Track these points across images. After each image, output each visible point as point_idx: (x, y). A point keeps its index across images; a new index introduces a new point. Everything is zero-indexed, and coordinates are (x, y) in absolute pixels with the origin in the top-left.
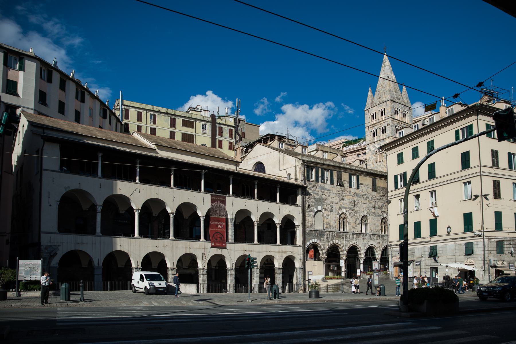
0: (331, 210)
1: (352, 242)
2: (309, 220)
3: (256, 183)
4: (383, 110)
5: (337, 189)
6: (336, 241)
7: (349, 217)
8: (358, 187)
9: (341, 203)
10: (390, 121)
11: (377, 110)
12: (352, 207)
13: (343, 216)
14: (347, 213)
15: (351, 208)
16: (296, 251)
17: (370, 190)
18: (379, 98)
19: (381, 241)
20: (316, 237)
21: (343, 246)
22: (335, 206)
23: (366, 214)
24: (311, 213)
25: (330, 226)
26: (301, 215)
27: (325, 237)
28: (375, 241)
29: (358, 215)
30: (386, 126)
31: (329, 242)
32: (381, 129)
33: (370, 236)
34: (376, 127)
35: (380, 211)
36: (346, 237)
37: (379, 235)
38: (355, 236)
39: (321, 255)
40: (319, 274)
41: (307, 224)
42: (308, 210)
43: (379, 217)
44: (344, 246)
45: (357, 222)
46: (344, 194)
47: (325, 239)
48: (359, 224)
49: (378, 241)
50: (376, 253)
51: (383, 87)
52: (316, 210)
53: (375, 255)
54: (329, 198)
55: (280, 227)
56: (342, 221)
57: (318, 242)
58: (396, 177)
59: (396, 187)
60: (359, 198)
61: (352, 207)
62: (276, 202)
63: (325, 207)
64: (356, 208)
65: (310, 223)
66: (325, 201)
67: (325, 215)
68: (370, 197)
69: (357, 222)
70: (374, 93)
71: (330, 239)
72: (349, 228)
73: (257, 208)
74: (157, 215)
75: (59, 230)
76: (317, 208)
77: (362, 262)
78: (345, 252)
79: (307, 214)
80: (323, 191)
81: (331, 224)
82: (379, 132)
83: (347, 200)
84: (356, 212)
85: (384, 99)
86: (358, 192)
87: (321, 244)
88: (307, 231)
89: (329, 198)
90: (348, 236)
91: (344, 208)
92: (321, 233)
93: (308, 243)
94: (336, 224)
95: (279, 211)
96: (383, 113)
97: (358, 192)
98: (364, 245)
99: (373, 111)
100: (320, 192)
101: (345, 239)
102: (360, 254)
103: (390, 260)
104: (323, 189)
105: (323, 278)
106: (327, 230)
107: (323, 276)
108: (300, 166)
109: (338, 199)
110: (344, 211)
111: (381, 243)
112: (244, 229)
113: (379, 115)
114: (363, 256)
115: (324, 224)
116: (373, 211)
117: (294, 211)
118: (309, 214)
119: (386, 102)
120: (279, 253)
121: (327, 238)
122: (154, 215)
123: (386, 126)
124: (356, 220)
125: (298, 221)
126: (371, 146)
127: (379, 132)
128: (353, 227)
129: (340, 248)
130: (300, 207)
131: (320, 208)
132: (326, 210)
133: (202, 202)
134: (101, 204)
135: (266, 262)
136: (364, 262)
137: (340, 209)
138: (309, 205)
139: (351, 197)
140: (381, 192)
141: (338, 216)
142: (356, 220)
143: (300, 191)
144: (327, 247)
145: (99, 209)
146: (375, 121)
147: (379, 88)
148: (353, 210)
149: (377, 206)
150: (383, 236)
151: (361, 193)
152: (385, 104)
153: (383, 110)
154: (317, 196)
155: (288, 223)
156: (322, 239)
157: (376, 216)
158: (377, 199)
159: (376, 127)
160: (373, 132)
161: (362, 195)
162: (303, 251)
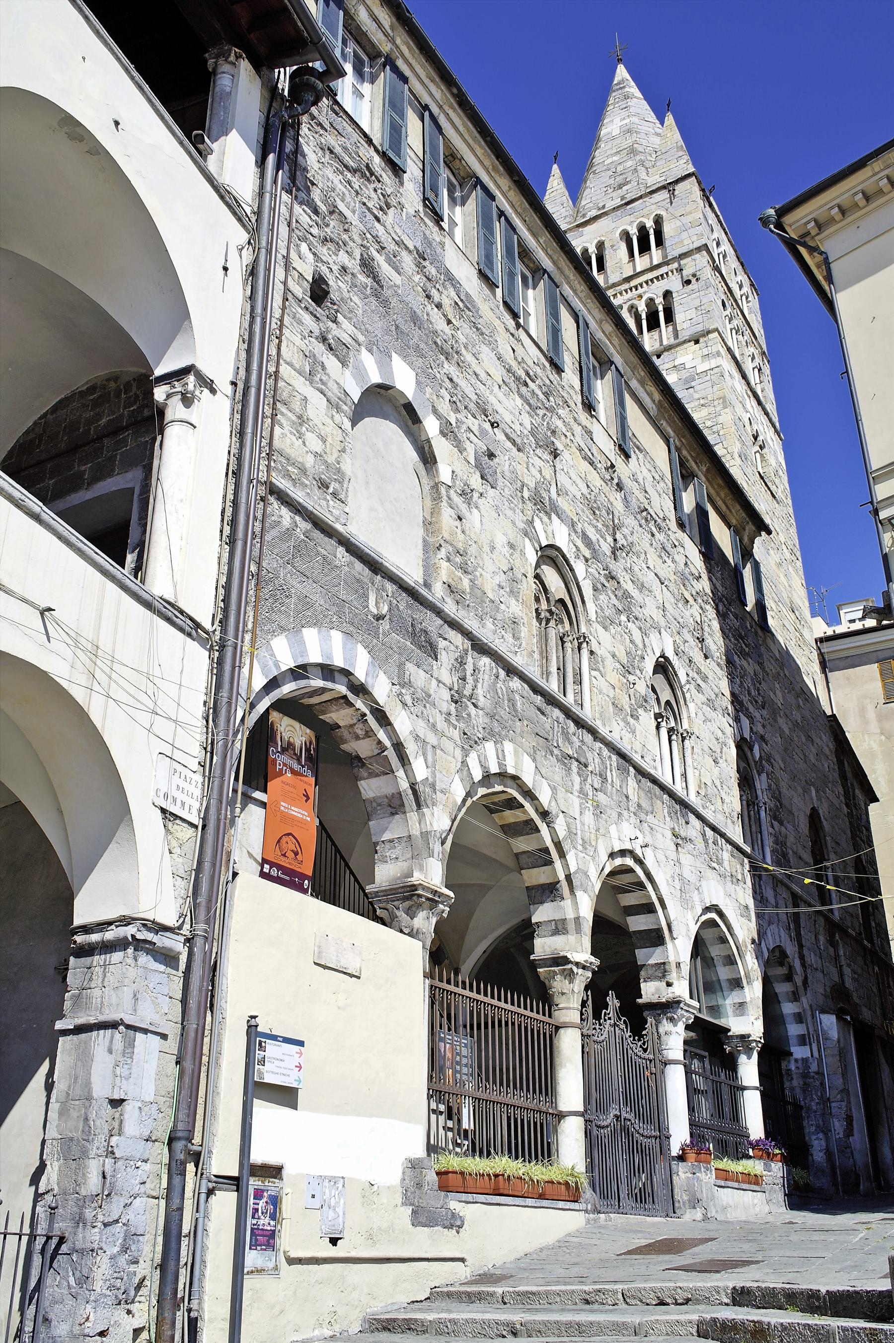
1: (623, 834)
4: (650, 224)
14: (580, 568)
18: (620, 187)
20: (364, 628)
24: (331, 362)
26: (236, 290)
27: (444, 668)
30: (673, 283)
31: (470, 742)
38: (632, 783)
40: (376, 1107)
63: (444, 407)
64: (617, 568)
70: (575, 187)
71: (479, 718)
78: (584, 906)
85: (655, 179)
93: (282, 653)
101: (577, 780)
110: (562, 538)
119: (669, 187)
123: (673, 283)
138: (319, 292)
144: (459, 792)
148: (611, 577)
153: (650, 224)
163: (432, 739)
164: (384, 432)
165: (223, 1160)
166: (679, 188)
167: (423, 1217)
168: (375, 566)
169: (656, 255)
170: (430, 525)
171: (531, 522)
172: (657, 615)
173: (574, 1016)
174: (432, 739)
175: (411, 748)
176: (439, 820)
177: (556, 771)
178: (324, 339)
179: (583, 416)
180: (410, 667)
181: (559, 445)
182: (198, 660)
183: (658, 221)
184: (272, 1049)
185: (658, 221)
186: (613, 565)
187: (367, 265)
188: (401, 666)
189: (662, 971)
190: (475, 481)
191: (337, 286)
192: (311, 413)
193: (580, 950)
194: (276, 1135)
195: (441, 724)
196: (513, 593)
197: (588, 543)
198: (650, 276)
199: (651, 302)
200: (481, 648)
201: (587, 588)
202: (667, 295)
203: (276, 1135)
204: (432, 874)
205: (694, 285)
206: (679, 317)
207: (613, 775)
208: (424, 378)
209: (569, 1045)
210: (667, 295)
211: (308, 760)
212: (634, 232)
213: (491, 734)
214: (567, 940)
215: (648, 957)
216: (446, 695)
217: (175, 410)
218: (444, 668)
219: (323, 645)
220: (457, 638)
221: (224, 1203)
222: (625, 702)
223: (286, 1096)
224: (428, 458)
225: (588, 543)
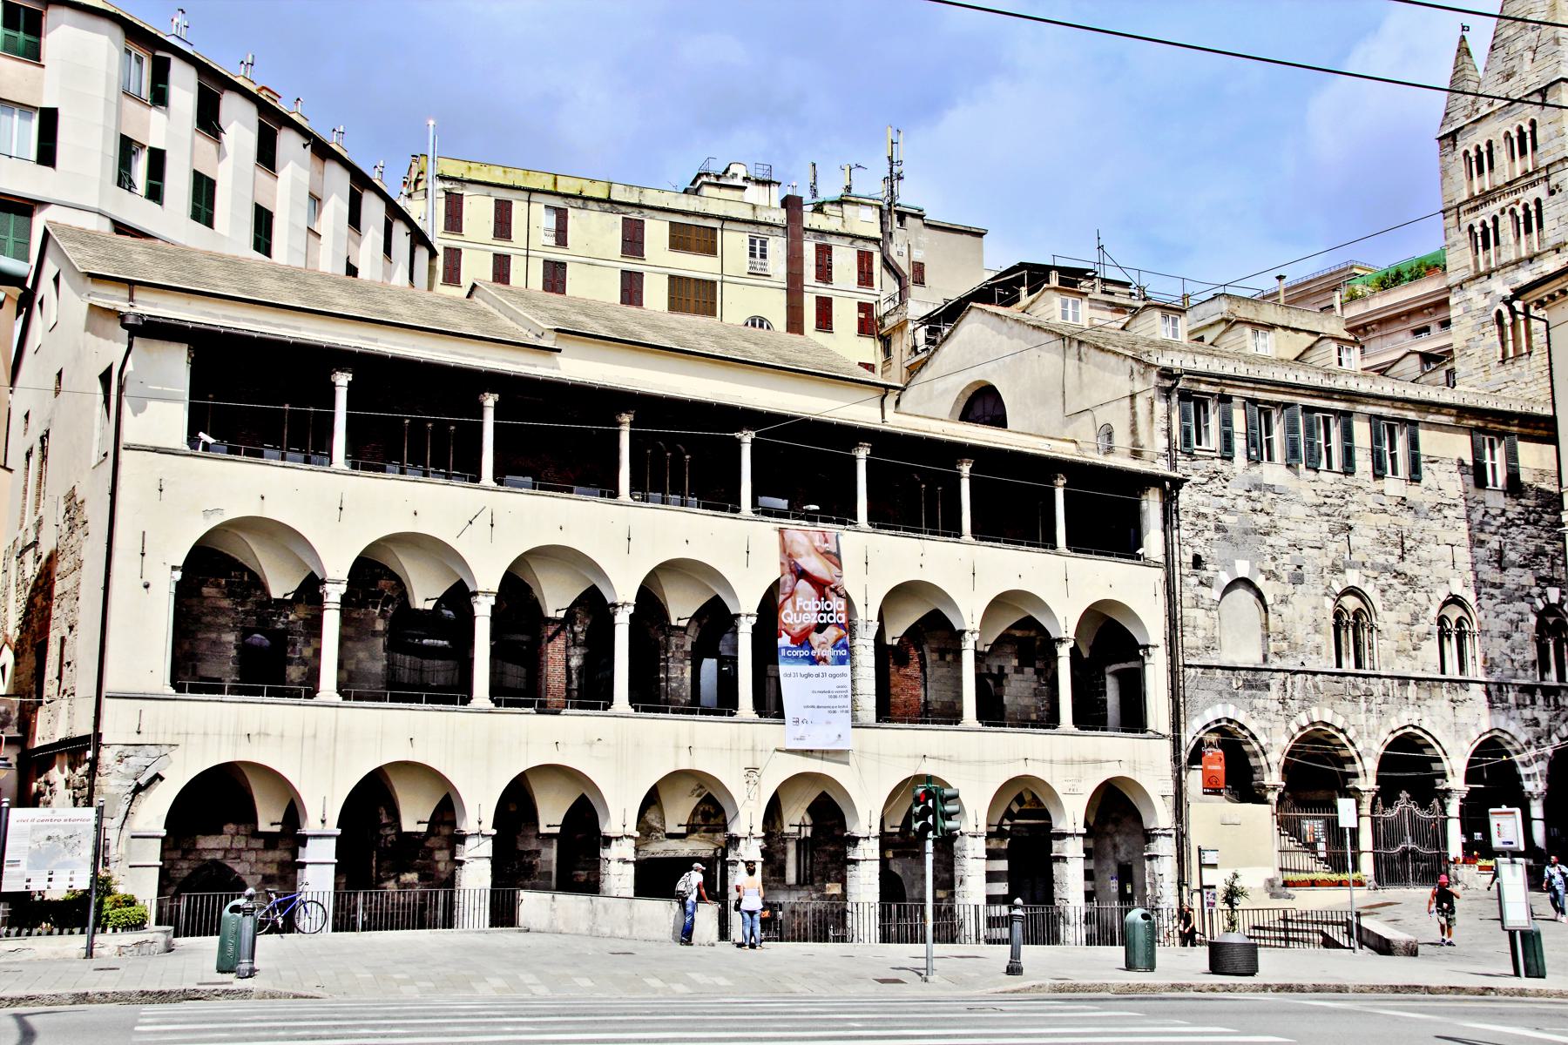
0: (1297, 579)
1: (1401, 718)
5: (1319, 486)
7: (1378, 606)
8: (1415, 475)
12: (1393, 560)
13: (1351, 603)
14: (1369, 589)
15: (1385, 569)
18: (1508, 77)
22: (1313, 561)
24: (1204, 591)
25: (1293, 646)
27: (1275, 692)
28: (1515, 713)
29: (1421, 597)
31: (1290, 717)
32: (1520, 212)
33: (1488, 693)
34: (1494, 208)
35: (1528, 578)
36: (1368, 695)
37: (1528, 690)
41: (1189, 640)
42: (1194, 581)
43: (1524, 606)
45: (1421, 628)
46: (1352, 507)
47: (1276, 706)
49: (1527, 713)
52: (1226, 579)
55: (1074, 652)
56: (1351, 626)
57: (1241, 718)
60: (1423, 523)
61: (1393, 560)
62: (1054, 547)
64: (1408, 567)
65: (1201, 633)
66: (1269, 540)
69: (1421, 628)
72: (1385, 653)
73: (971, 574)
74: (561, 615)
75: (174, 684)
79: (1187, 594)
80: (1255, 494)
83: (1363, 537)
84: (1411, 582)
86: (1414, 493)
87: (1253, 726)
88: (1190, 672)
89: (1282, 524)
91: (1352, 566)
92: (1254, 679)
94: (1318, 638)
95: (1066, 584)
96: (1524, 142)
97: (1414, 493)
100: (1241, 502)
101: (1363, 705)
104: (1257, 487)
106: (1276, 663)
108: (1152, 393)
109: (1325, 527)
110: (1353, 578)
111: (1544, 724)
112: (915, 663)
113: (1501, 156)
117: (1130, 585)
120: (1071, 764)
121: (1283, 702)
122: (550, 613)
123: (1543, 195)
124: (1415, 619)
126: (1473, 291)
127: (1506, 222)
130: (1157, 565)
131: (1243, 569)
133: (742, 550)
134: (344, 575)
137: (1336, 569)
138: (1197, 562)
141: (1329, 604)
142: (1415, 619)
145: (334, 594)
148: (1398, 574)
149: (1512, 556)
150: (1549, 692)
151: (1432, 499)
154: (1227, 520)
155: (1109, 635)
156: (1259, 703)
157: (1509, 599)
161: (1438, 508)
162: (1176, 759)
163: (1268, 725)
167: (1272, 895)
168: (1233, 669)
170: (1266, 626)
174: (1268, 725)
177: (1347, 706)
178: (1201, 583)
180: (1256, 701)
182: (1166, 746)
183: (1533, 123)
185: (1533, 123)
186: (1400, 567)
192: (1199, 622)
194: (1210, 877)
195: (1273, 717)
198: (1524, 181)
202: (1538, 202)
203: (1210, 877)
205: (1558, 196)
210: (1538, 202)
212: (1514, 134)
218: (1275, 692)
220: (1281, 675)
221: (1197, 896)
223: (1214, 866)
224: (1260, 596)
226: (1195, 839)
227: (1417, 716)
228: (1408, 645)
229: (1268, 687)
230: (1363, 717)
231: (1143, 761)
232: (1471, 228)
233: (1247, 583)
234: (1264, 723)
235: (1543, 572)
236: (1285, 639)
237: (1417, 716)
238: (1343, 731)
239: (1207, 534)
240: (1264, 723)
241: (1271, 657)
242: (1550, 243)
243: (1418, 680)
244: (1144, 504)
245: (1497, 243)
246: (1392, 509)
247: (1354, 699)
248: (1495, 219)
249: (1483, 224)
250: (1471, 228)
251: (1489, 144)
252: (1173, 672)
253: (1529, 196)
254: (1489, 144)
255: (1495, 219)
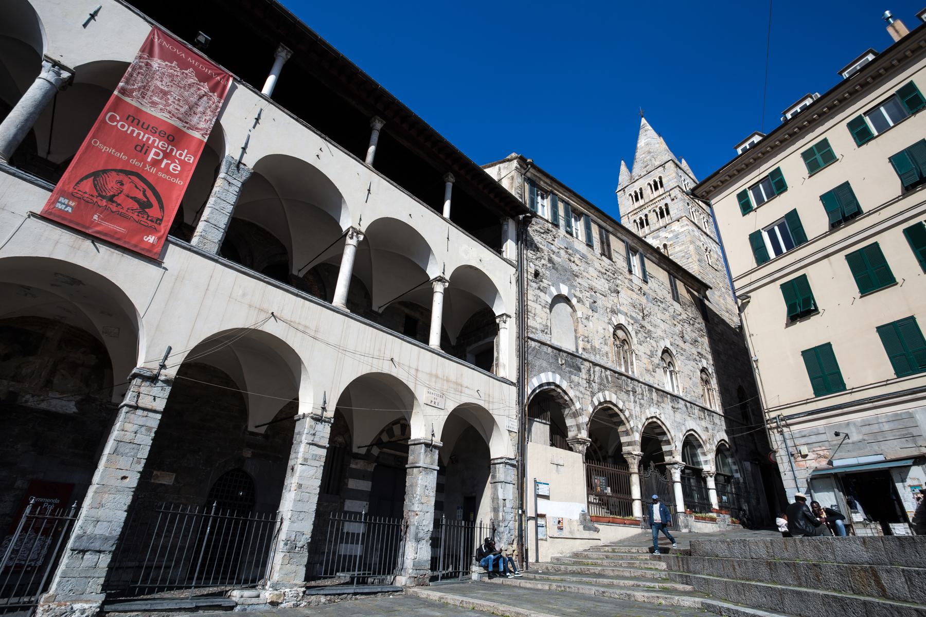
1: (652, 411)
2: (538, 318)
3: (378, 125)
4: (657, 180)
5: (603, 264)
6: (611, 396)
7: (635, 340)
8: (645, 281)
9: (613, 298)
10: (676, 192)
11: (643, 183)
14: (630, 328)
15: (636, 321)
16: (500, 400)
17: (669, 297)
19: (710, 427)
20: (558, 369)
21: (631, 415)
22: (601, 302)
23: (669, 346)
24: (542, 294)
25: (593, 349)
26: (514, 288)
27: (584, 374)
28: (698, 421)
30: (668, 200)
31: (593, 394)
34: (646, 211)
38: (654, 394)
39: (571, 434)
40: (572, 499)
42: (534, 285)
44: (636, 417)
47: (584, 383)
48: (658, 366)
49: (704, 424)
50: (702, 459)
51: (649, 152)
53: (699, 463)
54: (585, 274)
57: (565, 385)
58: (755, 239)
59: (761, 257)
60: (650, 305)
61: (640, 318)
63: (578, 294)
64: (645, 323)
67: (579, 314)
68: (671, 310)
70: (630, 168)
71: (595, 386)
76: (558, 289)
77: (677, 475)
78: (637, 437)
81: (597, 344)
82: (652, 217)
85: (657, 163)
87: (571, 393)
90: (639, 390)
92: (572, 361)
94: (606, 349)
95: (449, 248)
98: (678, 426)
99: (636, 187)
101: (632, 398)
102: (670, 453)
103: (783, 466)
105: (583, 514)
107: (584, 506)
108: (513, 173)
109: (607, 286)
110: (622, 320)
113: (647, 192)
114: (678, 458)
115: (576, 338)
116: (681, 344)
117: (498, 268)
118: (538, 297)
121: (589, 381)
123: (668, 200)
125: (504, 304)
127: (652, 217)
128: (647, 370)
129: (621, 423)
132: (580, 300)
135: (385, 438)
136: (682, 478)
137: (614, 312)
138: (537, 274)
139: (635, 296)
140: (689, 309)
143: (511, 227)
144: (591, 410)
146: (641, 202)
147: (640, 155)
148: (642, 327)
152: (661, 169)
153: (657, 180)
156: (575, 379)
157: (688, 359)
158: (683, 321)
159: (646, 211)
160: (638, 221)
163: (581, 396)
164: (562, 307)
165: (530, 513)
166: (667, 165)
168: (560, 350)
169: (661, 191)
170: (576, 330)
171: (610, 319)
172: (662, 334)
173: (636, 470)
174: (581, 396)
175: (574, 400)
176: (584, 419)
177: (623, 396)
178: (539, 288)
179: (628, 276)
180: (573, 377)
181: (619, 289)
182: (514, 390)
183: (660, 178)
184: (540, 486)
185: (660, 178)
186: (643, 323)
187: (550, 260)
188: (570, 377)
189: (670, 453)
190: (590, 313)
191: (542, 271)
192: (537, 312)
193: (637, 450)
194: (544, 507)
195: (584, 391)
196: (606, 344)
197: (632, 317)
199: (660, 208)
200: (595, 365)
201: (633, 334)
202: (666, 205)
203: (544, 507)
204: (584, 435)
206: (671, 212)
207: (646, 393)
208: (572, 287)
209: (635, 480)
210: (666, 205)
211: (545, 406)
212: (652, 183)
213: (600, 390)
214: (632, 447)
215: (665, 448)
216: (585, 382)
217: (502, 325)
218: (584, 374)
219: (546, 377)
220: (587, 364)
221: (531, 525)
222: (650, 368)
223: (546, 497)
224: (575, 311)
225: (632, 317)
226: (532, 473)
227: (658, 412)
228: (650, 368)
229: (579, 370)
230: (632, 404)
231: (500, 400)
232: (635, 221)
233: (567, 300)
234: (578, 394)
235: (699, 350)
236: (588, 342)
237: (658, 412)
238: (621, 410)
239: (543, 262)
240: (578, 394)
241: (580, 351)
242: (674, 219)
243: (657, 389)
244: (505, 227)
245: (648, 224)
246: (636, 290)
247: (627, 392)
248: (646, 215)
249: (641, 219)
250: (635, 221)
251: (641, 189)
252: (523, 339)
253: (662, 204)
254: (641, 189)
255: (646, 215)
